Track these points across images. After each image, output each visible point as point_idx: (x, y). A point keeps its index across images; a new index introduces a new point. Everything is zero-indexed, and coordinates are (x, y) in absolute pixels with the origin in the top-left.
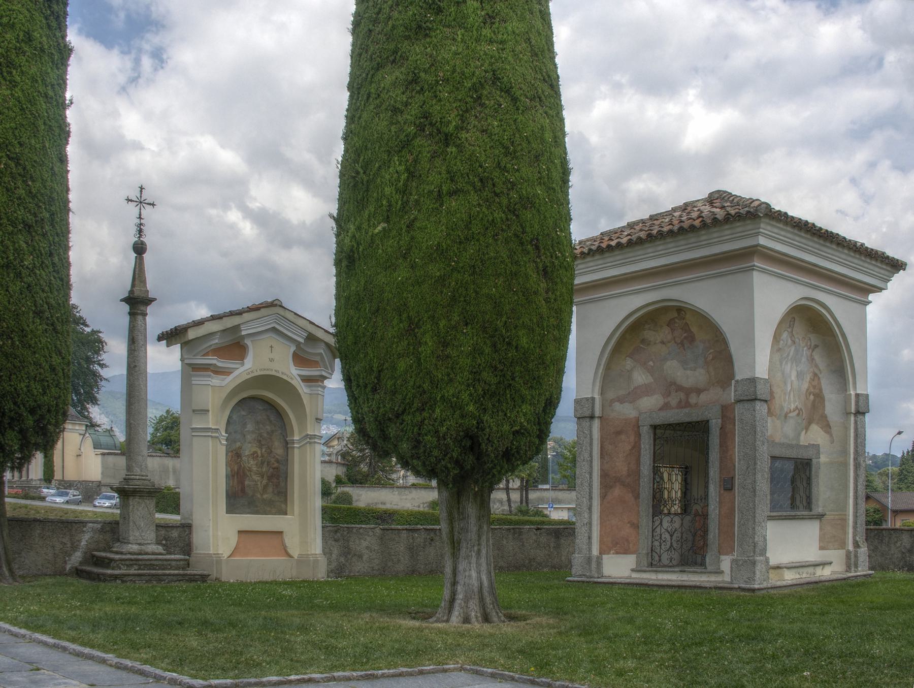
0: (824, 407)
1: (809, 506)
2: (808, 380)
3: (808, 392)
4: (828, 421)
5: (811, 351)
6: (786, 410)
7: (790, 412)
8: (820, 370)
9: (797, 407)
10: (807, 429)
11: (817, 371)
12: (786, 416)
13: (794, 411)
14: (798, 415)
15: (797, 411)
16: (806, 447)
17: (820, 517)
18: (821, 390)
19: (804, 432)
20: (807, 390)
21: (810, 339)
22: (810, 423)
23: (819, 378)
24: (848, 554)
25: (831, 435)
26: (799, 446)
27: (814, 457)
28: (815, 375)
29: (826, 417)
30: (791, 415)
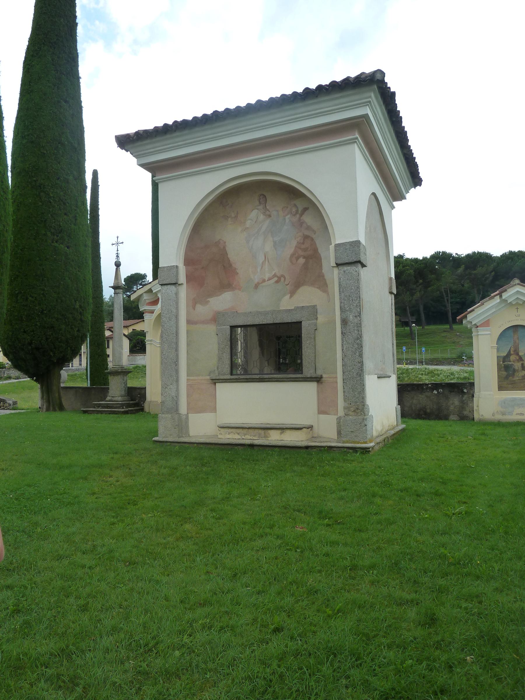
0: (321, 266)
1: (298, 368)
2: (294, 243)
3: (294, 257)
4: (325, 280)
5: (298, 216)
6: (256, 281)
7: (264, 281)
8: (313, 231)
9: (275, 276)
10: (292, 293)
11: (307, 233)
12: (256, 286)
13: (270, 279)
14: (277, 282)
15: (276, 279)
16: (289, 311)
17: (318, 380)
18: (316, 250)
19: (289, 296)
20: (292, 255)
21: (295, 205)
22: (297, 285)
23: (312, 239)
24: (339, 419)
25: (328, 294)
26: (279, 311)
27: (303, 319)
28: (306, 237)
29: (323, 276)
30: (264, 284)
